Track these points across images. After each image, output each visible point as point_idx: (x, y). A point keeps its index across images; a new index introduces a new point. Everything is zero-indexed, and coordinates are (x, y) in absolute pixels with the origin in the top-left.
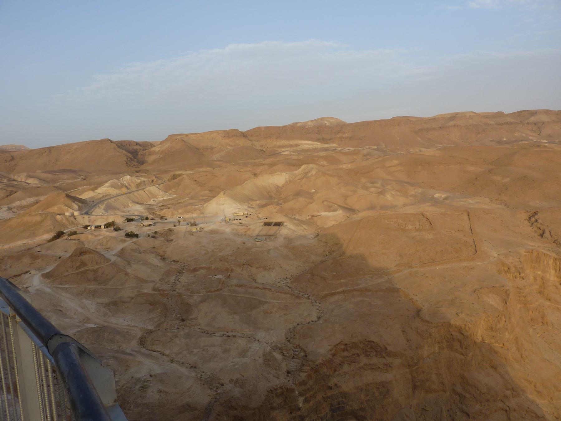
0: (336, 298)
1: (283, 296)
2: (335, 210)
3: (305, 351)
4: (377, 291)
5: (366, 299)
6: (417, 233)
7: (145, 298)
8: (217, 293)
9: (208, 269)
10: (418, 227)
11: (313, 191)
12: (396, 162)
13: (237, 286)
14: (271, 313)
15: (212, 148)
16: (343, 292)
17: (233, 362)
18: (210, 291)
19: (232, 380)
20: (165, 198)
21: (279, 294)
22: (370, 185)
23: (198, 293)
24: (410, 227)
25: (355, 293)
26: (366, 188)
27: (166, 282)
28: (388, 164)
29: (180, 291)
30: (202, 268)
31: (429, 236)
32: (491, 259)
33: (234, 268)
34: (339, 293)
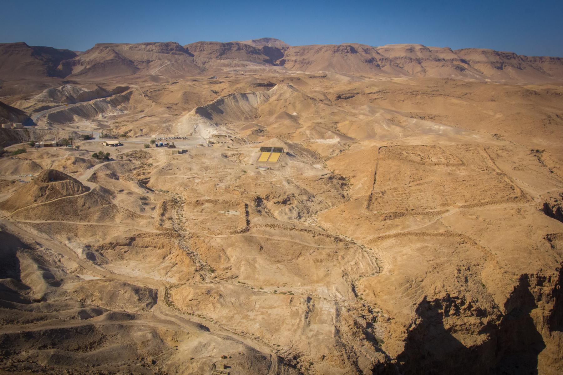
0: (389, 242)
1: (328, 240)
2: (330, 138)
3: (388, 312)
4: (435, 235)
5: (426, 244)
6: (446, 168)
7: (148, 239)
8: (245, 234)
9: (216, 202)
10: (443, 160)
11: (295, 114)
12: (376, 89)
13: (266, 226)
14: (321, 261)
15: (148, 62)
16: (397, 235)
17: (311, 330)
18: (235, 232)
19: (324, 356)
20: (115, 114)
21: (322, 237)
22: (357, 112)
23: (218, 234)
24: (435, 160)
25: (410, 237)
26: (354, 115)
27: (169, 219)
28: (367, 91)
29: (192, 231)
30: (207, 201)
31: (462, 173)
32: (535, 199)
33: (248, 203)
34: (389, 237)
